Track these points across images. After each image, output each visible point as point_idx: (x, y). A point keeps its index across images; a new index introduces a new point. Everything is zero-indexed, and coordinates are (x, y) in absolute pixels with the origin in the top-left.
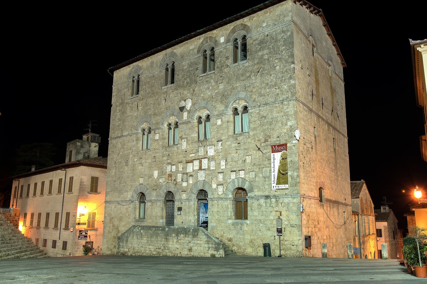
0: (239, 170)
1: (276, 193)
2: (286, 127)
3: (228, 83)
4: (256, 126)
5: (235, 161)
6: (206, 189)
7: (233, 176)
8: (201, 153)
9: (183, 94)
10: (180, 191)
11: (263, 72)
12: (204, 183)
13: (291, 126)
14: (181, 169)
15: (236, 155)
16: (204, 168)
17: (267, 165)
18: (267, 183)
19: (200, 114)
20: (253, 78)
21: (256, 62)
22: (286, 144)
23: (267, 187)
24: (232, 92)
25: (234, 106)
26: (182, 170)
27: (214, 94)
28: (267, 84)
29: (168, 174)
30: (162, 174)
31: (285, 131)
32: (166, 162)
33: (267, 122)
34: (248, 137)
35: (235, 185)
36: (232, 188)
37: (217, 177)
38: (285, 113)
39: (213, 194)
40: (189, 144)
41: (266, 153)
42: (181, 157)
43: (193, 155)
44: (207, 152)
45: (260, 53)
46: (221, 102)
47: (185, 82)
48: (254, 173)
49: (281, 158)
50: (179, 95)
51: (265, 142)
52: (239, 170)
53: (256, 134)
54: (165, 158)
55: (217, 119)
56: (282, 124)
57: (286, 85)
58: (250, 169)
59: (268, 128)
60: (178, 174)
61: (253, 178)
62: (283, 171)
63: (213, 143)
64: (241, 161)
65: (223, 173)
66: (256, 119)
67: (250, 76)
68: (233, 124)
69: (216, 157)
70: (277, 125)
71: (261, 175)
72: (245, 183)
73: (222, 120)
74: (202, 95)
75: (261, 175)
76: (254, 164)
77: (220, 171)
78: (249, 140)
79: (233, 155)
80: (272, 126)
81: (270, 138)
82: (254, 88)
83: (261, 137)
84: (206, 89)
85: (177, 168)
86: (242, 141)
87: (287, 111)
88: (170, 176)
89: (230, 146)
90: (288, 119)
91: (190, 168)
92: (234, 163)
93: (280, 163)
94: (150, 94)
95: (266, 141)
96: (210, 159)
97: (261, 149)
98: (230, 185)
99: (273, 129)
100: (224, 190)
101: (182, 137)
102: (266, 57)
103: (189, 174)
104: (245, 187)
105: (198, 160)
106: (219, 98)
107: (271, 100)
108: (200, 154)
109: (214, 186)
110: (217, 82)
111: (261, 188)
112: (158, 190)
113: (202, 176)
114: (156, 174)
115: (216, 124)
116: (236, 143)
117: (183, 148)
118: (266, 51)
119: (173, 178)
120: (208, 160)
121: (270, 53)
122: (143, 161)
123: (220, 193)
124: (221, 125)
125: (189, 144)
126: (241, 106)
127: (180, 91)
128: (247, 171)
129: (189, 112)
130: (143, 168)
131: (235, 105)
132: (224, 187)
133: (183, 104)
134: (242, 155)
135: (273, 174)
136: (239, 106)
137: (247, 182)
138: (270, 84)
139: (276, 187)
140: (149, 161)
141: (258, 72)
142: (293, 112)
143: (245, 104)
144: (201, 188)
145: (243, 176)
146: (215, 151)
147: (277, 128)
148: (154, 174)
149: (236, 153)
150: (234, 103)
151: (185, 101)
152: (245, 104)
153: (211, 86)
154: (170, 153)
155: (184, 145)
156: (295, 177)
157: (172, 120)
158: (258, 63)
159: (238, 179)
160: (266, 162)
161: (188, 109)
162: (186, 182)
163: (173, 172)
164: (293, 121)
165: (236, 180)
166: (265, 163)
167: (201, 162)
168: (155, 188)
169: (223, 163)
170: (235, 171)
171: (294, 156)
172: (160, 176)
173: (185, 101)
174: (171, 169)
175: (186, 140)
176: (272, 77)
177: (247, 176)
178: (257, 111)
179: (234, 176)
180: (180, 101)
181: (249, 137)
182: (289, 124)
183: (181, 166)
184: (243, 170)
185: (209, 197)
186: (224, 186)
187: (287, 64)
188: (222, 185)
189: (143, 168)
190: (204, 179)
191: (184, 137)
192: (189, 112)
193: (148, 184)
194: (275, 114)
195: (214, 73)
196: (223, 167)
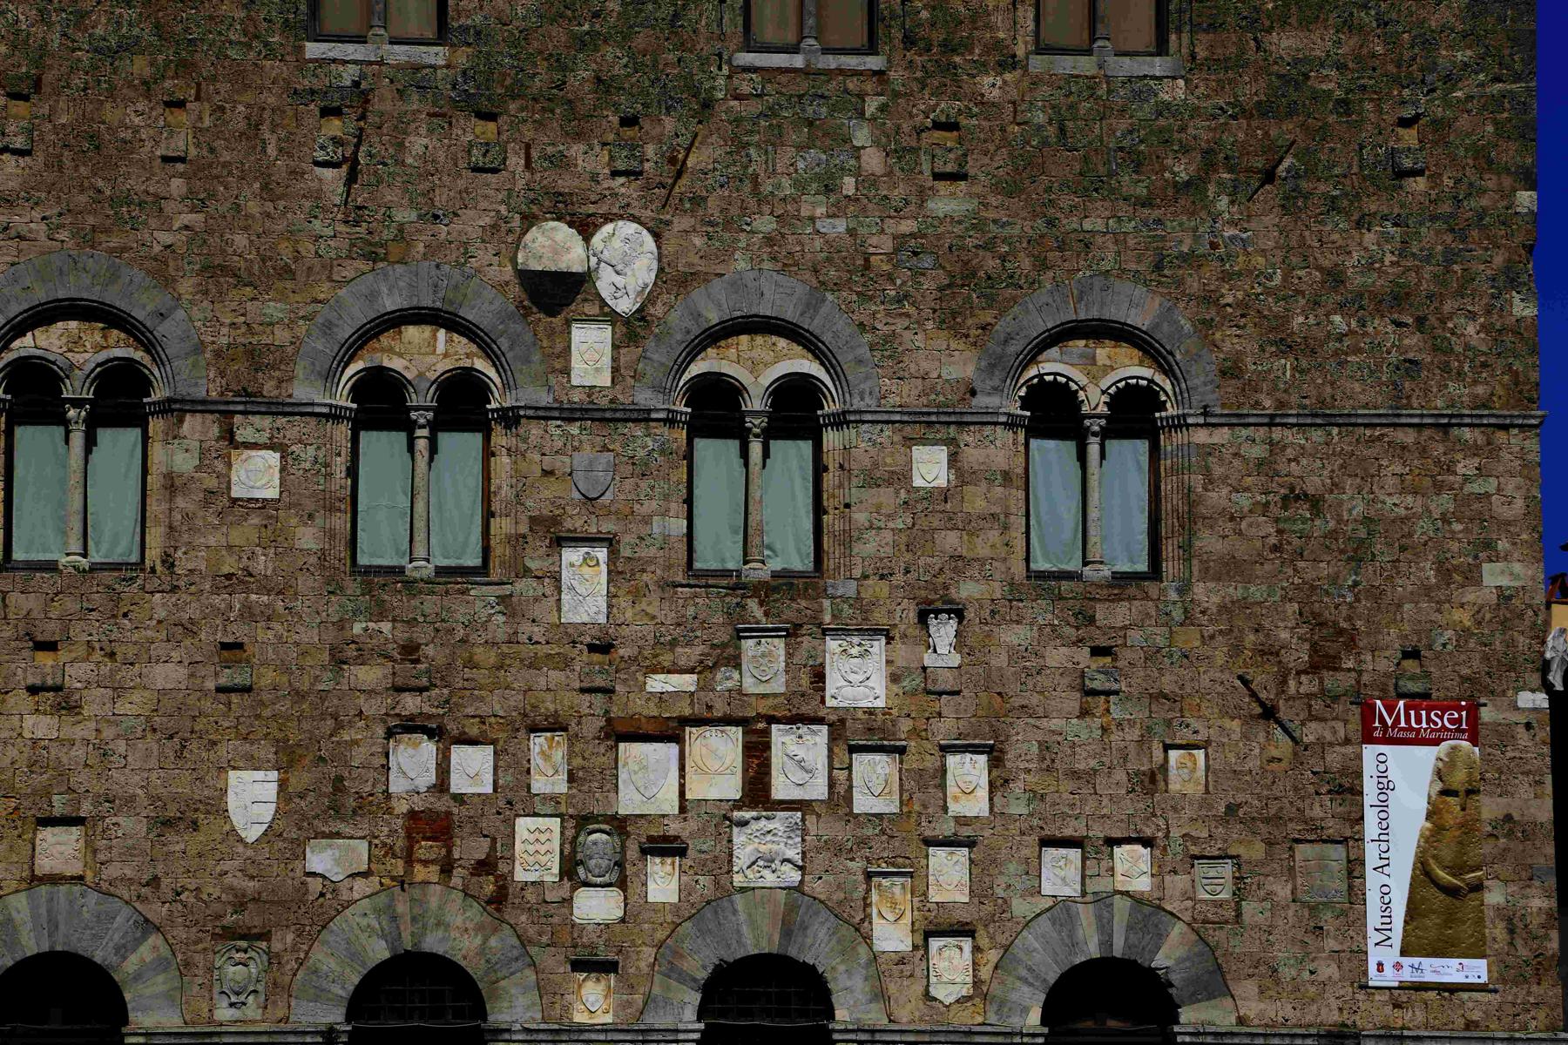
0: (1112, 842)
1: (1399, 1018)
2: (1470, 595)
3: (1010, 189)
4: (1242, 550)
5: (1074, 774)
6: (818, 948)
7: (1060, 873)
8: (764, 668)
9: (560, 162)
10: (554, 962)
11: (1304, 185)
12: (791, 908)
13: (1504, 596)
14: (549, 779)
15: (1084, 731)
16: (796, 794)
17: (1333, 828)
18: (1331, 944)
19: (727, 368)
20: (1223, 202)
21: (1250, 90)
22: (1474, 710)
23: (1328, 970)
24: (1042, 265)
25: (1047, 367)
26: (561, 787)
27: (887, 245)
28: (1335, 277)
29: (402, 807)
30: (326, 796)
31: (1464, 617)
32: (372, 707)
33: (1333, 535)
34: (1177, 614)
35: (1074, 945)
36: (1045, 959)
37: (915, 875)
38: (1463, 501)
40: (637, 595)
41: (1323, 745)
42: (556, 688)
43: (687, 682)
44: (819, 677)
45: (1284, 43)
46: (951, 322)
47: (583, 74)
48: (1227, 870)
49: (1439, 786)
50: (516, 161)
51: (1314, 668)
53: (1244, 604)
54: (369, 675)
55: (909, 442)
56: (1445, 572)
57: (1472, 316)
58: (1195, 840)
59: (1334, 580)
60: (524, 825)
61: (1219, 904)
62: (1457, 869)
63: (879, 617)
64: (1120, 775)
65: (970, 844)
66: (1244, 501)
67: (1193, 186)
68: (1021, 494)
69: (905, 725)
70: (1403, 566)
71: (1283, 891)
72: (1160, 937)
73: (953, 460)
74: (765, 224)
75: (1283, 891)
76: (1231, 809)
77: (947, 829)
78: (1190, 639)
79: (1056, 723)
80: (1368, 575)
81: (1351, 643)
82: (1226, 277)
83: (1284, 635)
84: (801, 186)
85: (511, 765)
86: (1135, 636)
87: (1468, 488)
88: (434, 824)
89: (1028, 663)
90: (1488, 545)
91: (647, 780)
92: (1067, 785)
93: (1429, 817)
94: (140, 66)
95: (1321, 662)
96: (853, 735)
97: (1283, 714)
98: (1028, 938)
99: (1376, 594)
101: (555, 521)
102: (1330, 83)
103: (639, 834)
104: (1161, 960)
105: (737, 733)
106: (928, 284)
107: (1360, 392)
108: (750, 686)
109: (892, 935)
110: (899, 153)
111: (1287, 973)
112: (283, 940)
113: (765, 853)
114: (252, 798)
115: (902, 477)
116: (1079, 642)
117: (569, 616)
118: (1320, 42)
119: (470, 849)
120: (833, 739)
121: (1358, 59)
122: (77, 674)
123: (945, 993)
124: (945, 495)
125: (637, 595)
126: (1104, 384)
127: (528, 133)
128: (1176, 848)
129: (631, 330)
130: (79, 732)
131: (1052, 365)
132: (976, 949)
133: (554, 246)
134: (1136, 734)
135: (1373, 880)
136: (1094, 379)
137: (1178, 930)
138: (1359, 280)
139: (1398, 966)
140: (168, 675)
141: (1269, 176)
142: (1519, 503)
143: (1147, 372)
144: (754, 936)
145: (1143, 884)
146: (894, 678)
147: (1404, 587)
148: (232, 802)
149: (1084, 713)
150: (1054, 352)
151: (586, 228)
152: (1147, 372)
153: (857, 173)
154: (422, 634)
155: (584, 588)
156: (1535, 922)
157: (422, 357)
158: (1264, 110)
159: (1103, 901)
160: (1321, 809)
161: (625, 306)
162: (615, 895)
163: (460, 799)
164: (1517, 567)
166: (1317, 812)
167: (757, 754)
168: (252, 919)
169: (968, 775)
171: (1524, 790)
172: (298, 823)
173: (586, 228)
174: (443, 769)
175: (602, 554)
176: (1369, 238)
177: (1179, 882)
178: (1258, 451)
179: (1073, 873)
180: (529, 220)
181: (1188, 619)
182: (1494, 576)
183: (559, 755)
184: (1147, 842)
185: (841, 1014)
186: (983, 941)
187: (1490, 182)
188: (963, 930)
189: (79, 732)
190: (795, 876)
191: (575, 522)
192: (631, 330)
193: (155, 882)
194: (1394, 503)
195: (880, 73)
196: (976, 805)
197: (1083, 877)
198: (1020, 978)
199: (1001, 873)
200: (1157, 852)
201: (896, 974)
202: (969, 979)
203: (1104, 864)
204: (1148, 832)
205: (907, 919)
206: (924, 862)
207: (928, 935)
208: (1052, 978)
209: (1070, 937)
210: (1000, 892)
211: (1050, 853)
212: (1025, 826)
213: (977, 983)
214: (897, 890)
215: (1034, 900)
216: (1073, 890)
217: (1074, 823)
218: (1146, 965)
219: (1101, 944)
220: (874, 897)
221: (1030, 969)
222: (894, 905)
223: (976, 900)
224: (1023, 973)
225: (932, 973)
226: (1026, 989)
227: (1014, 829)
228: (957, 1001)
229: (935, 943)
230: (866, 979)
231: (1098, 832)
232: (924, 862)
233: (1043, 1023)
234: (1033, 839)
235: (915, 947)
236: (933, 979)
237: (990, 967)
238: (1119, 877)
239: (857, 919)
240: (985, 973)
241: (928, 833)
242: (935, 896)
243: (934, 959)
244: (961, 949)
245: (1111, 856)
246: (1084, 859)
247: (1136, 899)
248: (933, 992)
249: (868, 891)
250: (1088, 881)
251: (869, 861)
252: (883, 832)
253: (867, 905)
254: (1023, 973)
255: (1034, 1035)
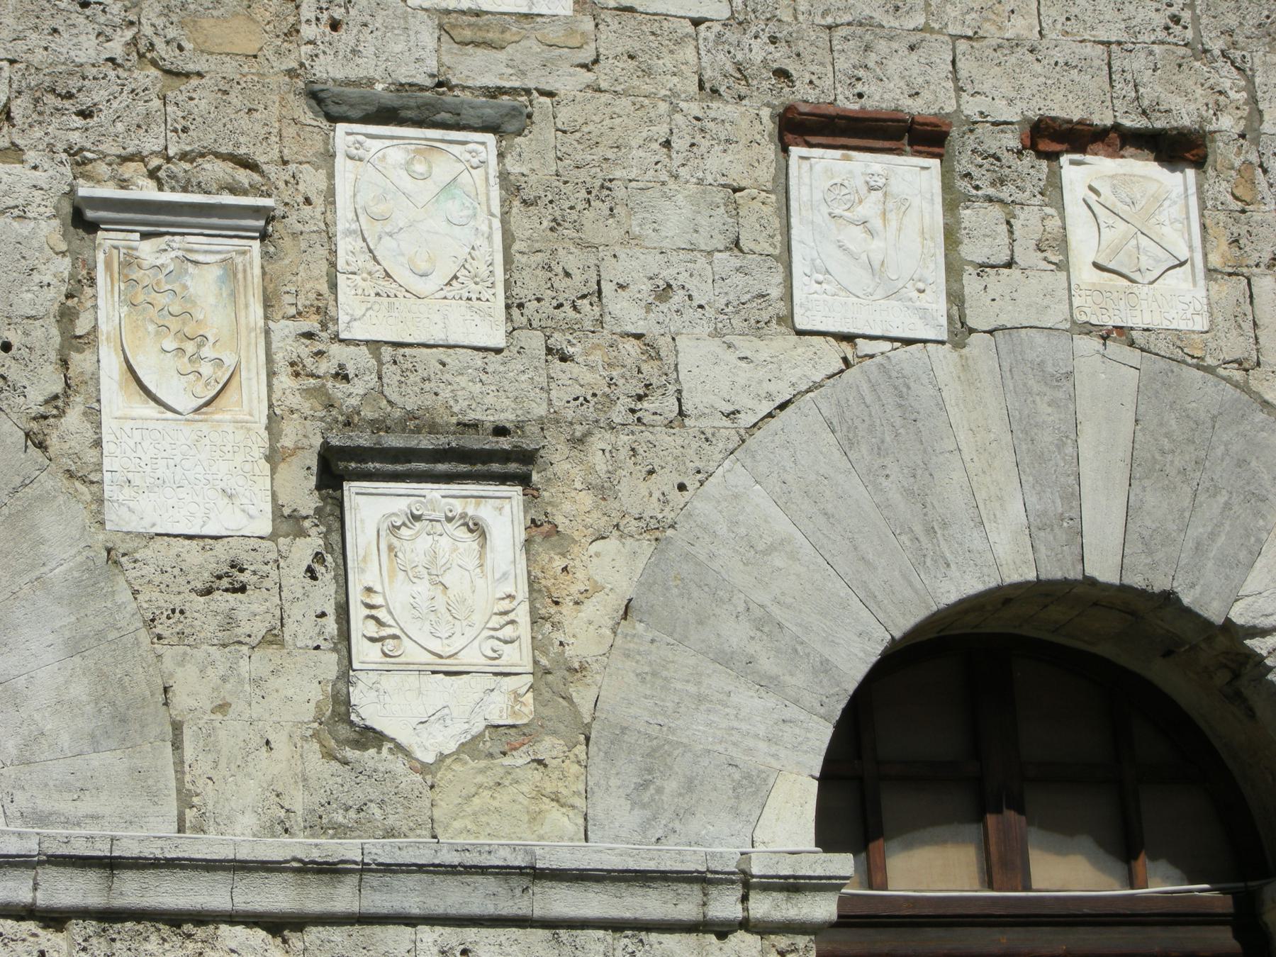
7: (868, 237)
39: (144, 717)
52: (1054, 138)
65: (503, 117)
100: (584, 631)
123: (415, 712)
132: (541, 531)
165: (966, 399)
170: (924, 136)
184: (1177, 148)
186: (572, 505)
188: (493, 458)
197: (953, 269)
198: (724, 659)
199: (630, 238)
200: (1220, 189)
201: (209, 627)
202: (518, 656)
203: (1029, 221)
204: (1183, 113)
205: (250, 399)
206: (312, 181)
207: (334, 470)
208: (855, 659)
209: (918, 496)
210: (626, 311)
211: (817, 167)
212: (717, 64)
213: (553, 674)
214: (204, 285)
215: (764, 349)
216: (928, 315)
217: (901, 64)
218: (1213, 612)
219: (1035, 528)
220: (107, 309)
221: (765, 624)
222: (192, 341)
223: (535, 342)
224: (736, 634)
225: (357, 613)
226: (748, 700)
227: (680, 65)
228: (470, 747)
229: (369, 506)
230: (75, 648)
231: (1003, 97)
232: (312, 181)
233: (827, 839)
234: (753, 119)
235: (288, 522)
236: (364, 653)
237: (600, 610)
238: (1084, 274)
239: (35, 398)
240: (584, 631)
241: (329, 69)
242: (361, 316)
243: (365, 573)
244: (477, 529)
245: (1053, 190)
246: (953, 201)
247: (1179, 354)
248: (370, 707)
249: (81, 282)
250: (971, 284)
251: (79, 159)
252: (142, 52)
253: (74, 341)
254: (736, 634)
255: (793, 886)
